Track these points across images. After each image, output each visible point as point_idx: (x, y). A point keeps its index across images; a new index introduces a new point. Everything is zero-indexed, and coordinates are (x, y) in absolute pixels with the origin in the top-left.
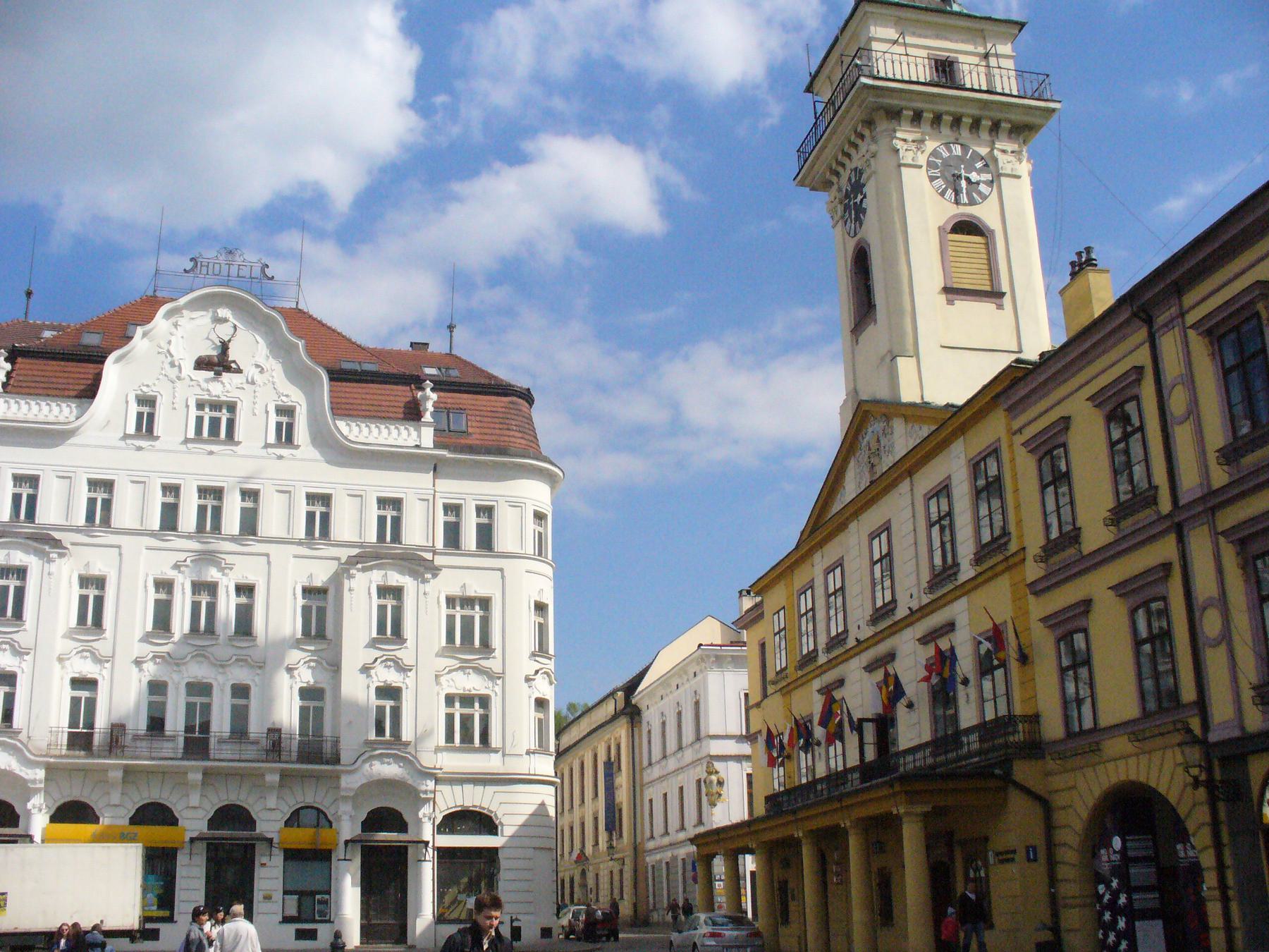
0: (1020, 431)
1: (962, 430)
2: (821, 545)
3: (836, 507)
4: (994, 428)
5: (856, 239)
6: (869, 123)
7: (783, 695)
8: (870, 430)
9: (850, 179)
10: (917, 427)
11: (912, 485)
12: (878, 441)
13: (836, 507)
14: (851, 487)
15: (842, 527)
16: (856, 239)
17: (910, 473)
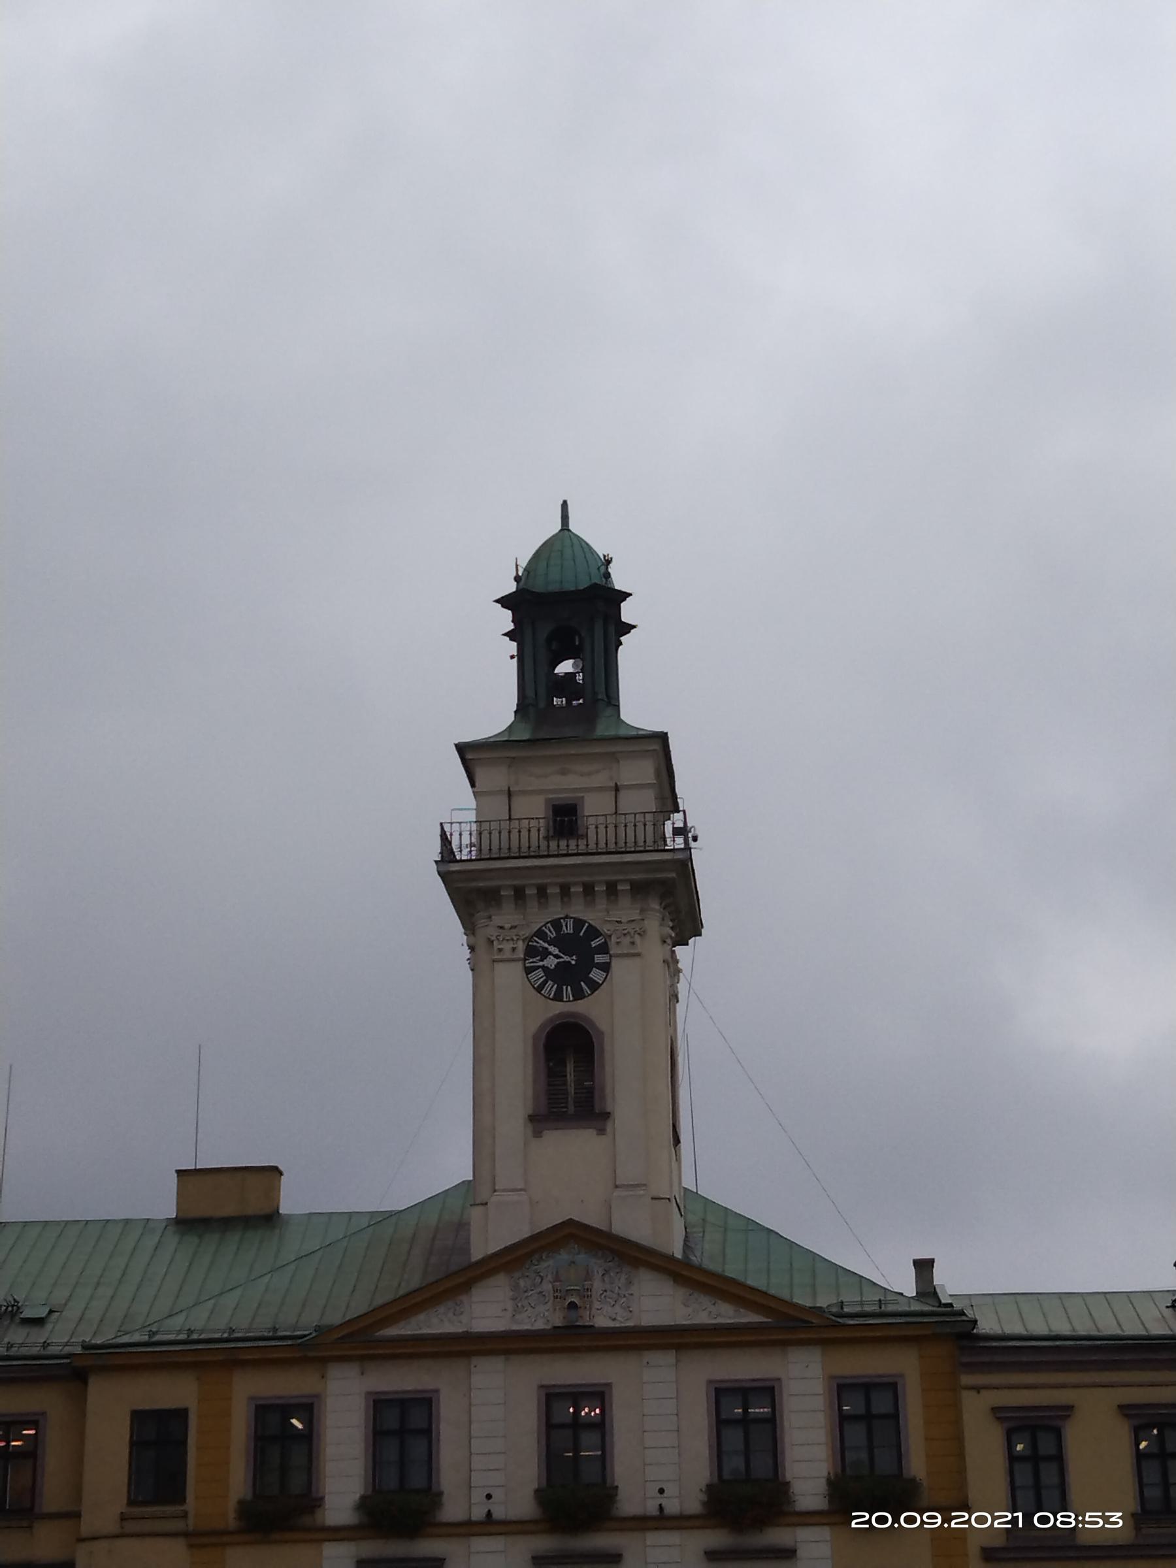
0: (978, 1389)
1: (823, 1343)
2: (362, 1358)
3: (438, 1322)
4: (904, 1365)
5: (558, 1008)
6: (639, 890)
7: (191, 1546)
8: (564, 1256)
9: (556, 924)
10: (706, 1300)
11: (677, 1361)
12: (588, 1276)
13: (438, 1322)
14: (489, 1310)
15: (467, 1355)
16: (558, 1008)
17: (679, 1348)
